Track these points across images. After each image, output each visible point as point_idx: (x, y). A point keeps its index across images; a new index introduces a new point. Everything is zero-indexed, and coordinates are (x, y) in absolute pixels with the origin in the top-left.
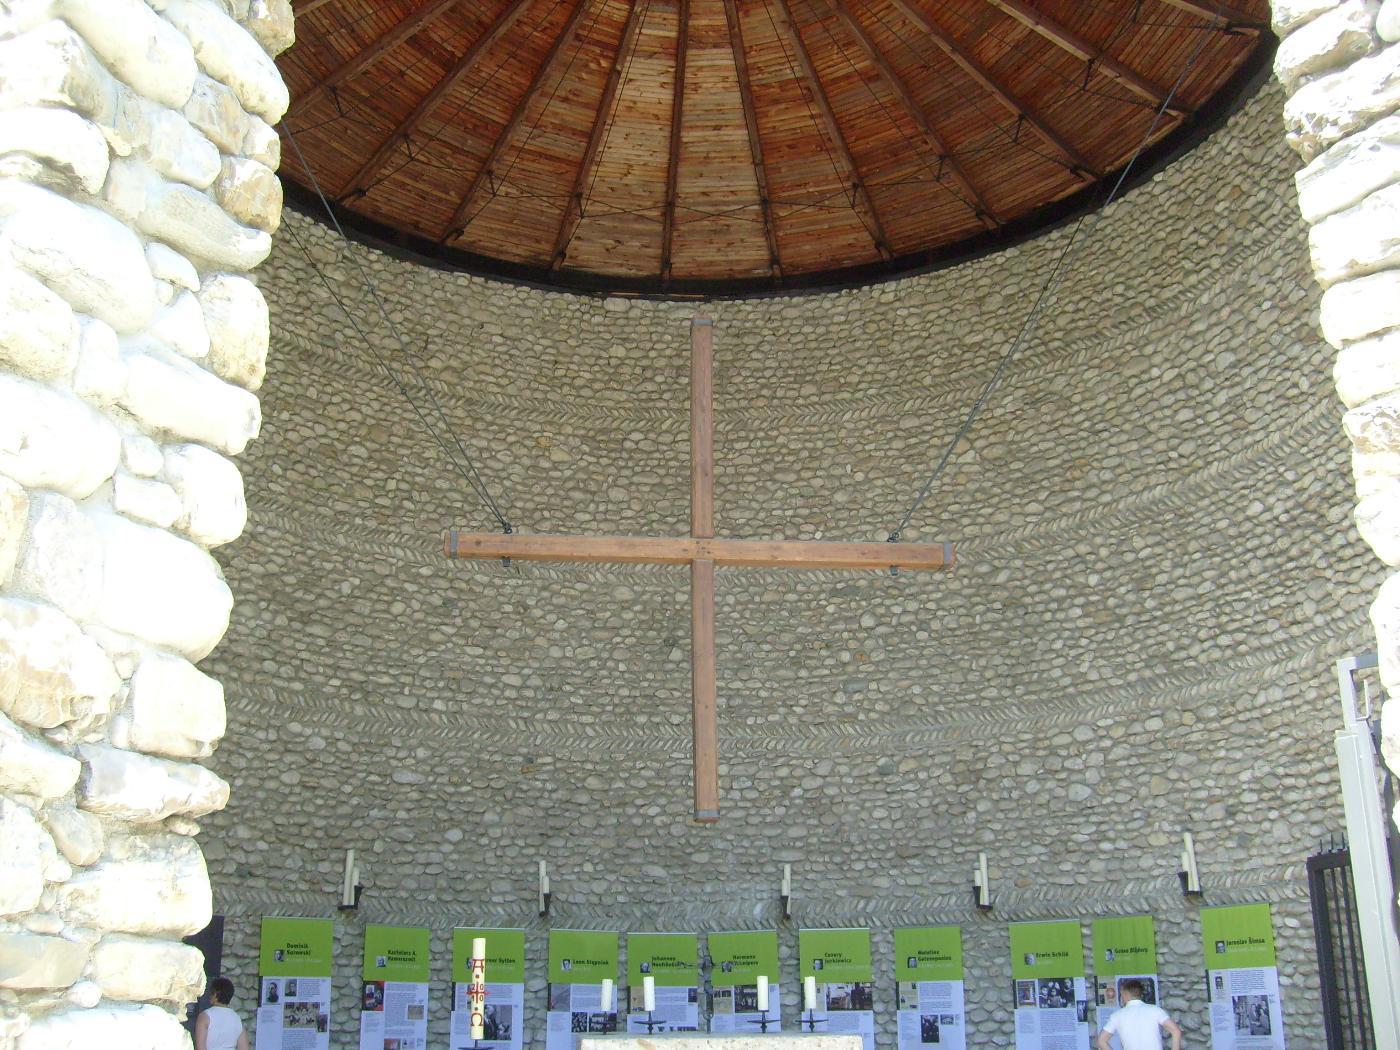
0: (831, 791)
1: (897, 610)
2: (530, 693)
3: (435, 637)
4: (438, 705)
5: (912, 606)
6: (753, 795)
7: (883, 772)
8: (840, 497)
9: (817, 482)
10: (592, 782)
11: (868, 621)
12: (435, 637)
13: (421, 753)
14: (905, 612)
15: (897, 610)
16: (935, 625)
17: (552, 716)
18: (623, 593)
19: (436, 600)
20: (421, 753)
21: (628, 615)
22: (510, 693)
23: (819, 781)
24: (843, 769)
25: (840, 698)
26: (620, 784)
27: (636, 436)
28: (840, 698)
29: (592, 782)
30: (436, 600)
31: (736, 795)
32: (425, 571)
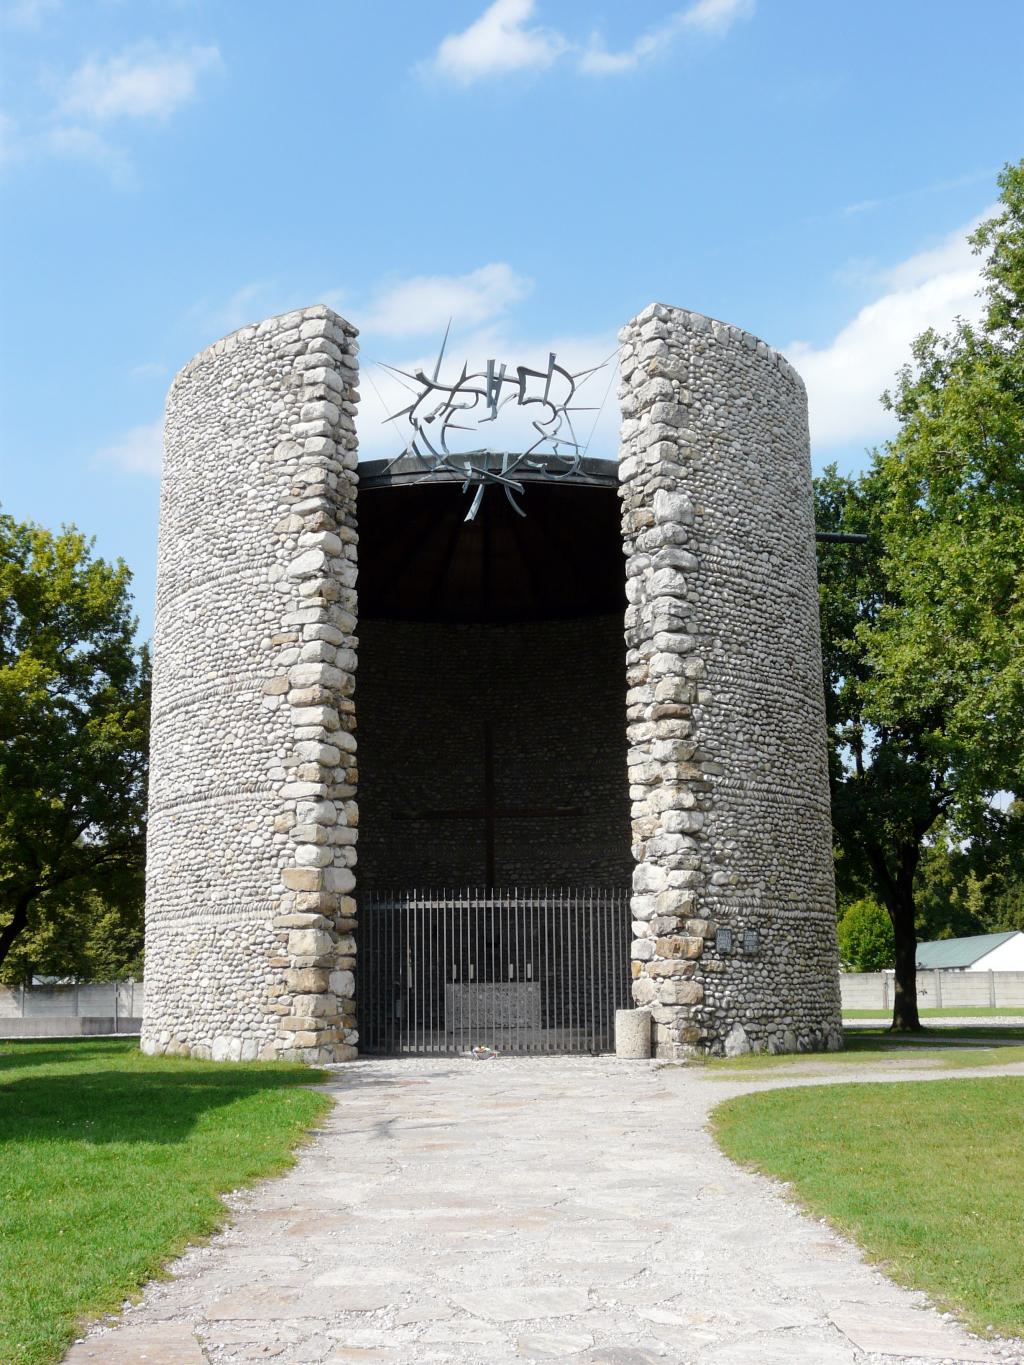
0: (570, 875)
1: (601, 788)
2: (425, 831)
3: (380, 807)
4: (382, 840)
5: (608, 786)
6: (532, 877)
7: (593, 866)
8: (575, 730)
9: (564, 722)
10: (455, 873)
11: (587, 793)
12: (380, 807)
13: (375, 863)
14: (605, 789)
15: (601, 788)
16: (618, 796)
17: (435, 842)
18: (469, 780)
19: (379, 790)
20: (375, 863)
21: (471, 791)
22: (416, 832)
23: (563, 871)
24: (575, 865)
25: (574, 831)
26: (469, 873)
27: (473, 698)
28: (574, 831)
29: (455, 873)
30: (379, 790)
31: (524, 877)
32: (372, 776)
